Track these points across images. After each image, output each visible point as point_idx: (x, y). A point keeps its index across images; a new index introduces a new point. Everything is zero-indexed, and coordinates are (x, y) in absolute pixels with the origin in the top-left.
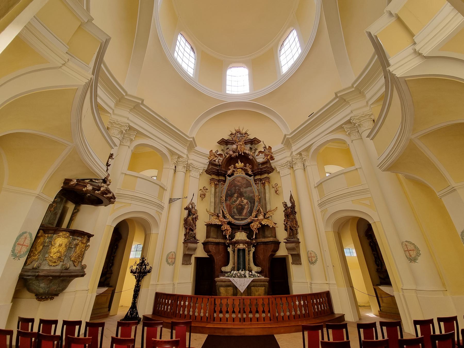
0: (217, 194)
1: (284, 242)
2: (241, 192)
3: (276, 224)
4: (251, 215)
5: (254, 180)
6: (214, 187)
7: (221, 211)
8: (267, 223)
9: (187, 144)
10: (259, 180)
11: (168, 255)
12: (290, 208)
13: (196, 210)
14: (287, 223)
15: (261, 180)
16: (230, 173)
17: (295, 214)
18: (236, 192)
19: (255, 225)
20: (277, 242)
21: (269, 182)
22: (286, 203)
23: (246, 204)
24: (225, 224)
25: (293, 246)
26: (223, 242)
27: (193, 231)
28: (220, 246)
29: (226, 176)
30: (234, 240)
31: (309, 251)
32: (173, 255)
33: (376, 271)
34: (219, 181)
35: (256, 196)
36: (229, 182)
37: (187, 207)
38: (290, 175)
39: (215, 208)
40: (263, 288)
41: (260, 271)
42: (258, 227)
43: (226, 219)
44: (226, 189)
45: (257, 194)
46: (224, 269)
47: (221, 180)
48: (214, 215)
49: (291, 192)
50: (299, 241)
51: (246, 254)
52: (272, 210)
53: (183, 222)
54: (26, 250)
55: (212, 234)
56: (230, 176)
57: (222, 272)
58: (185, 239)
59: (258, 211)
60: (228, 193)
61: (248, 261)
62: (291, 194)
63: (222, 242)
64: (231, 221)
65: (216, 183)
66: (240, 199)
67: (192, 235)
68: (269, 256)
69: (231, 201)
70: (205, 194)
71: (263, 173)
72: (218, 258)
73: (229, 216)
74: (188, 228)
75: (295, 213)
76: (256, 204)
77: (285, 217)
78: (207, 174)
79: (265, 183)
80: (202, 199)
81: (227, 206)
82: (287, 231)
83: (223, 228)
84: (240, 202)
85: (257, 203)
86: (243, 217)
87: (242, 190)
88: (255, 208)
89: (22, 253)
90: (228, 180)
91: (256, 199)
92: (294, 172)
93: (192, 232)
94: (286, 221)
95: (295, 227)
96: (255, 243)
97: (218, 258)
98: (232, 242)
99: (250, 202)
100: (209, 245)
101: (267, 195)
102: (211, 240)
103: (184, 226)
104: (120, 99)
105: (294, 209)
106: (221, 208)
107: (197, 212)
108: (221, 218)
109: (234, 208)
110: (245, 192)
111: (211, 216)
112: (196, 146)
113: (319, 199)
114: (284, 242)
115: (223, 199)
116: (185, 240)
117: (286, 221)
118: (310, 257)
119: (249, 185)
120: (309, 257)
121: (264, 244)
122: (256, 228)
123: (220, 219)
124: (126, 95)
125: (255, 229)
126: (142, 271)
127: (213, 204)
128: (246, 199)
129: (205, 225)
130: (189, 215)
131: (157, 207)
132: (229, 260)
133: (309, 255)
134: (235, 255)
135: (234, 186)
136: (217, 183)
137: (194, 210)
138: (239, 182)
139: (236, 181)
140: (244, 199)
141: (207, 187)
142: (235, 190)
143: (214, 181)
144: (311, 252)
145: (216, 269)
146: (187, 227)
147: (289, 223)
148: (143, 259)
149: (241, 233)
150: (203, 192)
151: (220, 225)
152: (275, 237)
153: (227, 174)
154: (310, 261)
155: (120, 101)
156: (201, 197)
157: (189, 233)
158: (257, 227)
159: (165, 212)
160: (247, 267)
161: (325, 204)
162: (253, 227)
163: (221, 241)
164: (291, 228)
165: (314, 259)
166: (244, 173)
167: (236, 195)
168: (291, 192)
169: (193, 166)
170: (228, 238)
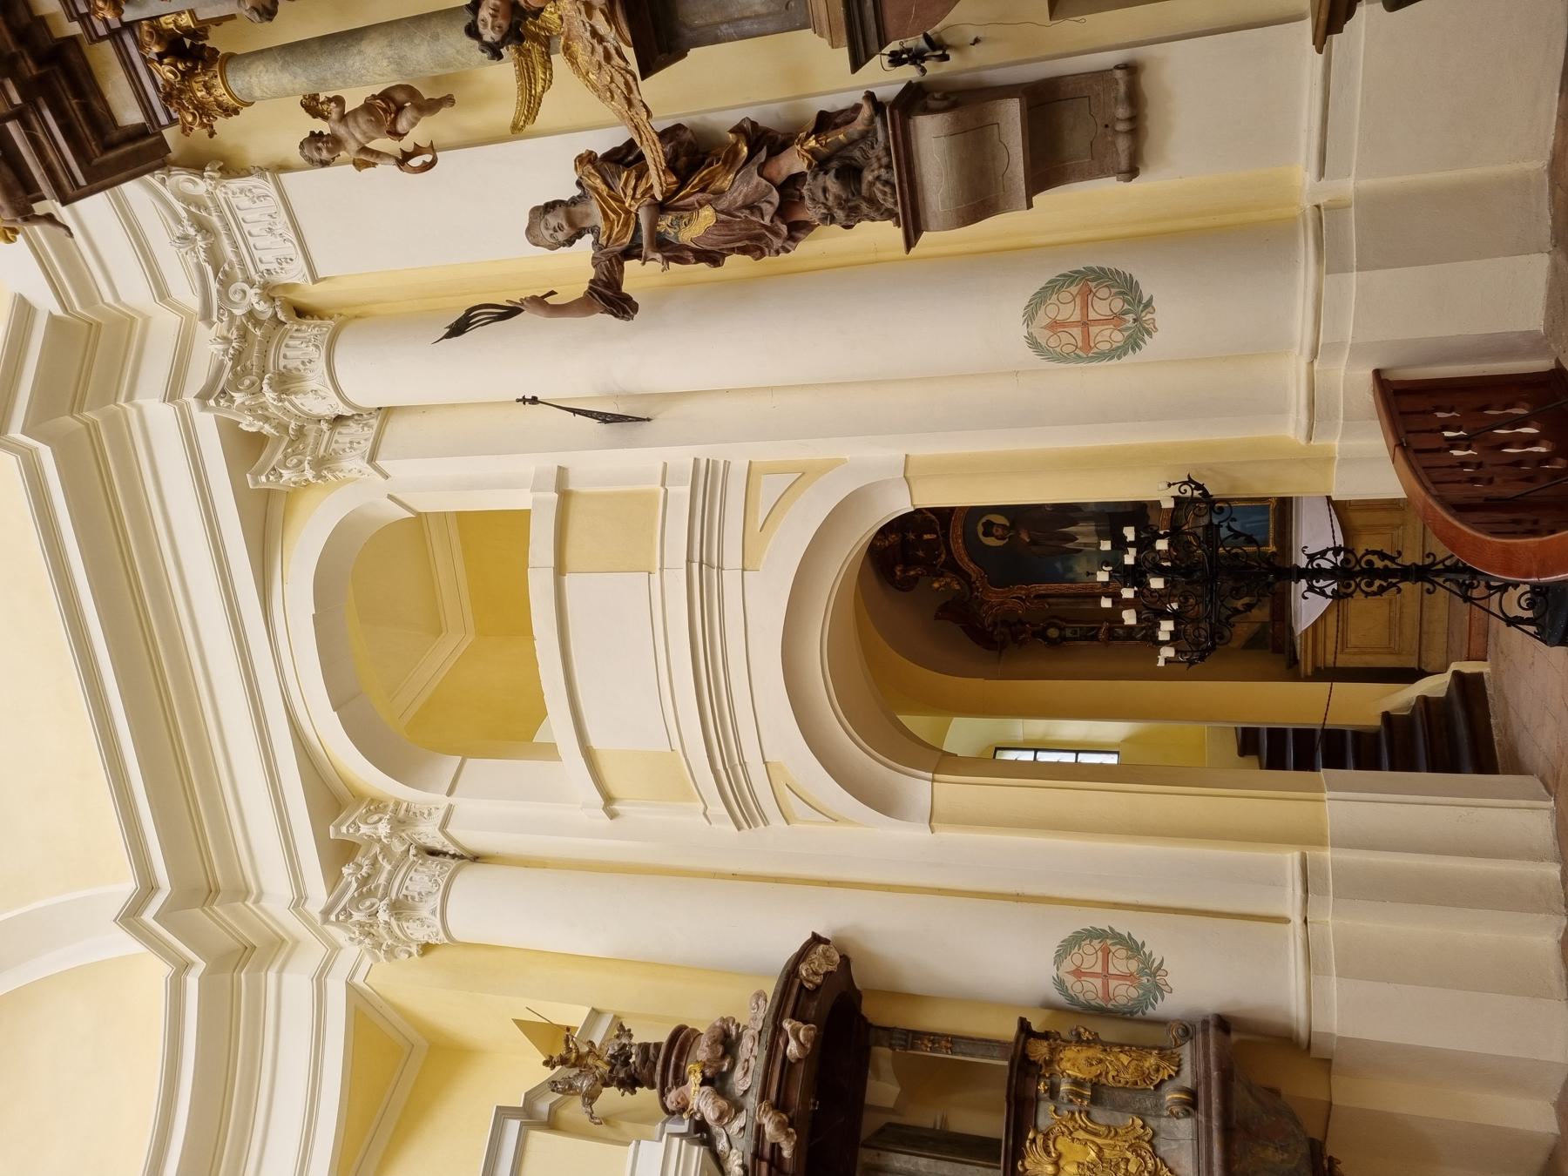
9: (92, 429)
32: (1055, 326)
104: (239, 965)
112: (24, 311)
124: (186, 966)
131: (720, 568)
155: (248, 949)
169: (214, 286)
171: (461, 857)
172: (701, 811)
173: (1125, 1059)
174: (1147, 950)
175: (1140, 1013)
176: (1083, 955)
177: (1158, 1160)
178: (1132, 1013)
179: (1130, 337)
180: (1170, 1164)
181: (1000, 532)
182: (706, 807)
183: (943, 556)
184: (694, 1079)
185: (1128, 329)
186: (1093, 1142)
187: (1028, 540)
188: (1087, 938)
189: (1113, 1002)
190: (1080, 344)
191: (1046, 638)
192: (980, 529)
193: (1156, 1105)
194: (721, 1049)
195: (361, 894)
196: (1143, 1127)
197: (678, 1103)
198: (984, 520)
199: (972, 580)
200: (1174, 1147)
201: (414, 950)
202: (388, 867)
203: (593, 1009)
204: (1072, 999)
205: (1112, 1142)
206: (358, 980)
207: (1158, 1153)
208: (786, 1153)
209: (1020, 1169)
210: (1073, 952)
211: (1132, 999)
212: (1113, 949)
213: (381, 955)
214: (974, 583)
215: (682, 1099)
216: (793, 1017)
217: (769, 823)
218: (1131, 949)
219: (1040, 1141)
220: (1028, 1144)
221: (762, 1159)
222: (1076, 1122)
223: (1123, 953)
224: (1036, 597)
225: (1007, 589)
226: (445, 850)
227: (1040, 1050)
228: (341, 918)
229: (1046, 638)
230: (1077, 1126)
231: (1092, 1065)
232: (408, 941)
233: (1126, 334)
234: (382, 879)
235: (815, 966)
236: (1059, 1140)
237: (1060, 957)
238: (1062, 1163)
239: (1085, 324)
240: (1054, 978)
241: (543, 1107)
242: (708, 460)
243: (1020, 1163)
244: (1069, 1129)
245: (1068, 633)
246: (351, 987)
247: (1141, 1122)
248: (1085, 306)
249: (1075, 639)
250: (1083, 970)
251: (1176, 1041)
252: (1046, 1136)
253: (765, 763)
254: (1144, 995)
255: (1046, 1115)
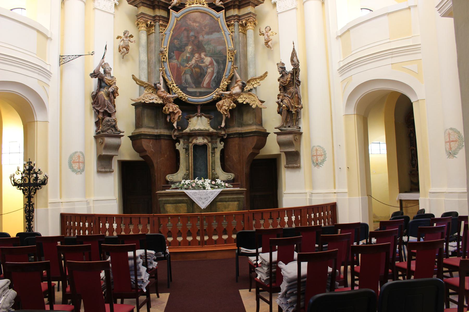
0: (153, 45)
1: (275, 133)
2: (199, 41)
3: (262, 102)
4: (218, 85)
5: (226, 18)
6: (145, 32)
7: (161, 78)
8: (247, 101)
10: (236, 18)
11: (71, 157)
12: (290, 74)
13: (113, 77)
14: (282, 101)
15: (239, 18)
16: (177, 3)
17: (298, 86)
18: (189, 41)
19: (225, 104)
20: (263, 132)
21: (255, 24)
22: (283, 64)
23: (209, 65)
24: (170, 102)
25: (290, 139)
26: (168, 134)
27: (110, 115)
28: (162, 141)
29: (170, 7)
30: (187, 130)
31: (314, 146)
32: (79, 157)
33: (409, 174)
34: (154, 18)
35: (229, 50)
36: (175, 22)
37: (95, 72)
38: (295, 10)
39: (149, 73)
40: (236, 203)
41: (232, 179)
42: (231, 108)
43: (170, 94)
44: (171, 35)
45: (230, 46)
46: (169, 177)
47: (159, 17)
48: (149, 85)
49: (293, 43)
50: (299, 131)
51: (209, 154)
52: (257, 76)
53: (89, 101)
55: (146, 121)
56: (177, 9)
57: (167, 182)
58: (98, 130)
59: (232, 78)
60: (174, 44)
61: (212, 163)
62: (294, 49)
63: (165, 134)
64: (181, 97)
65: (149, 23)
66: (197, 55)
67: (109, 123)
68: (247, 155)
69: (180, 59)
70: (128, 46)
71: (245, 4)
72: (159, 160)
73: (176, 87)
74: (100, 111)
75: (298, 84)
76: (229, 65)
77: (280, 90)
78: (131, 4)
79: (246, 24)
80: (123, 56)
81: (172, 69)
82: (281, 115)
83: (167, 110)
84: (198, 60)
85: (230, 63)
86: (202, 90)
87: (201, 38)
88: (226, 73)
90: (174, 17)
91: (228, 56)
92: (303, 4)
93: (108, 118)
94: (281, 97)
95: (296, 107)
96: (224, 135)
97: (159, 160)
98: (183, 133)
99: (217, 62)
100: (143, 140)
101: (250, 49)
102: (144, 130)
103: (94, 108)
105: (298, 76)
106: (161, 74)
107: (114, 81)
108: (162, 91)
109: (186, 72)
110: (208, 42)
111: (142, 88)
113: (342, 60)
114: (275, 133)
115: (165, 56)
116: (98, 131)
117: (281, 97)
118: (315, 156)
119: (216, 28)
120: (313, 156)
121: (241, 136)
122: (227, 108)
123: (159, 92)
125: (226, 110)
126: (32, 182)
127: (145, 66)
128: (210, 57)
129: (133, 105)
130: (100, 86)
131: (39, 74)
132: (179, 164)
133: (314, 152)
134: (189, 155)
135: (185, 29)
136: (152, 23)
137: (108, 77)
138: (195, 21)
139: (190, 20)
140: (206, 56)
141: (132, 30)
142: (188, 37)
143: (145, 19)
144: (318, 148)
145: (156, 178)
146: (98, 109)
147: (285, 101)
148: (29, 164)
149: (199, 118)
150: (124, 43)
151: (161, 104)
152: (261, 124)
153: (170, 5)
154: (315, 161)
156: (120, 51)
157: (103, 119)
158: (228, 108)
159: (54, 82)
160: (211, 173)
161: (350, 68)
162: (221, 107)
163: (164, 132)
164: (289, 109)
165: (320, 159)
166: (205, 3)
167: (189, 48)
168: (293, 43)
170: (176, 127)
179: (76, 170)
185: (77, 170)
190: (75, 161)
233: (76, 170)
239: (79, 162)
242: (51, 76)
248: (82, 162)
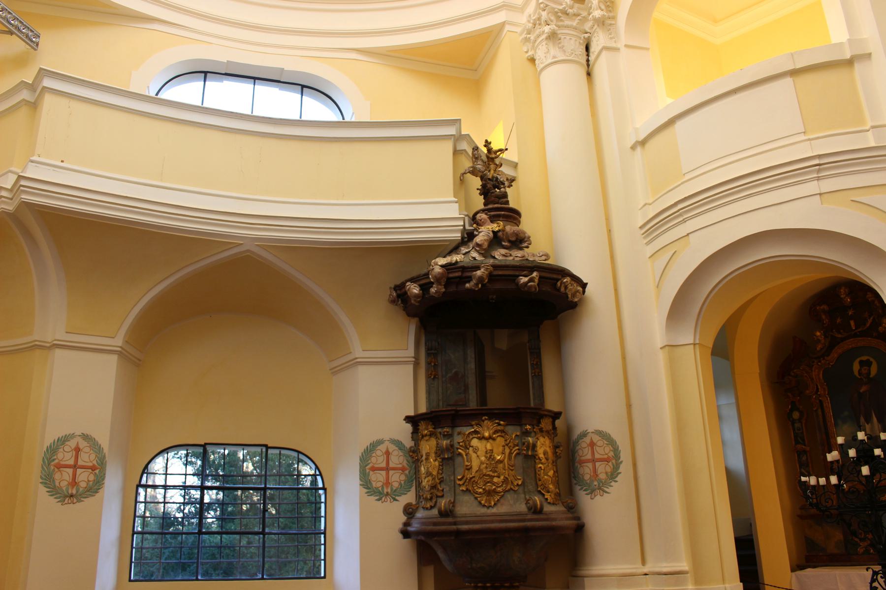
54: (403, 477)
89: (396, 485)
131: (818, 179)
171: (588, 65)
172: (647, 202)
173: (551, 473)
174: (613, 483)
175: (575, 482)
176: (603, 447)
177: (502, 494)
178: (574, 477)
180: (502, 501)
181: (864, 371)
182: (650, 204)
183: (840, 336)
184: (495, 227)
186: (505, 457)
187: (861, 391)
188: (614, 448)
189: (579, 466)
191: (791, 411)
192: (864, 358)
193: (530, 492)
194: (513, 239)
195: (557, 13)
196: (518, 485)
197: (481, 220)
198: (872, 360)
199: (826, 358)
200: (511, 501)
201: (530, 53)
202: (575, 24)
203: (517, 164)
204: (576, 442)
205: (507, 468)
206: (507, 28)
207: (507, 493)
208: (467, 285)
209: (483, 418)
210: (604, 440)
211: (583, 476)
212: (610, 464)
213: (524, 36)
214: (824, 359)
215: (483, 222)
216: (540, 277)
217: (647, 245)
218: (612, 474)
219: (499, 428)
220: (497, 421)
221: (463, 272)
222: (513, 448)
223: (609, 470)
224: (820, 401)
225: (823, 381)
226: (591, 54)
227: (546, 424)
228: (542, 5)
229: (791, 411)
230: (511, 448)
231: (544, 454)
232: (534, 48)
234: (568, 22)
235: (570, 287)
236: (502, 438)
237: (599, 433)
238: (491, 441)
240: (586, 431)
241: (464, 146)
243: (487, 418)
244: (509, 444)
245: (797, 425)
246: (503, 24)
247: (520, 483)
249: (794, 430)
250: (594, 447)
251: (565, 502)
252: (503, 431)
253: (688, 235)
254: (587, 483)
255: (513, 431)
